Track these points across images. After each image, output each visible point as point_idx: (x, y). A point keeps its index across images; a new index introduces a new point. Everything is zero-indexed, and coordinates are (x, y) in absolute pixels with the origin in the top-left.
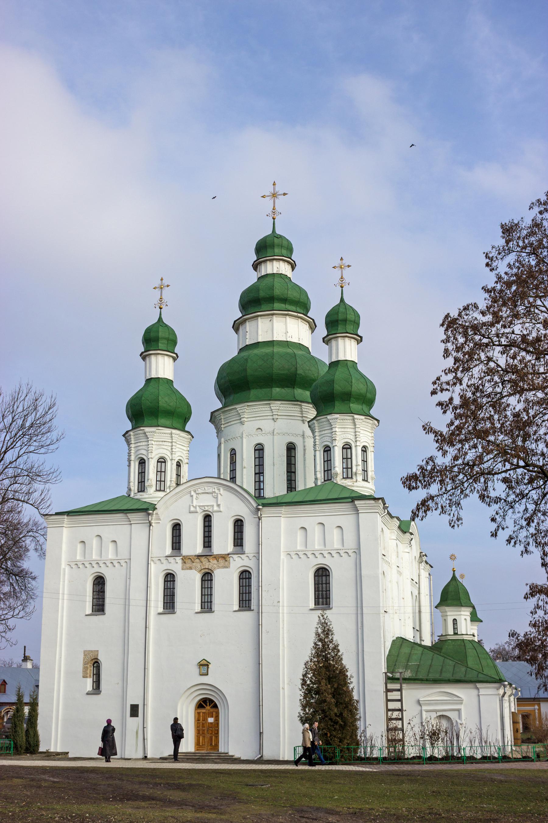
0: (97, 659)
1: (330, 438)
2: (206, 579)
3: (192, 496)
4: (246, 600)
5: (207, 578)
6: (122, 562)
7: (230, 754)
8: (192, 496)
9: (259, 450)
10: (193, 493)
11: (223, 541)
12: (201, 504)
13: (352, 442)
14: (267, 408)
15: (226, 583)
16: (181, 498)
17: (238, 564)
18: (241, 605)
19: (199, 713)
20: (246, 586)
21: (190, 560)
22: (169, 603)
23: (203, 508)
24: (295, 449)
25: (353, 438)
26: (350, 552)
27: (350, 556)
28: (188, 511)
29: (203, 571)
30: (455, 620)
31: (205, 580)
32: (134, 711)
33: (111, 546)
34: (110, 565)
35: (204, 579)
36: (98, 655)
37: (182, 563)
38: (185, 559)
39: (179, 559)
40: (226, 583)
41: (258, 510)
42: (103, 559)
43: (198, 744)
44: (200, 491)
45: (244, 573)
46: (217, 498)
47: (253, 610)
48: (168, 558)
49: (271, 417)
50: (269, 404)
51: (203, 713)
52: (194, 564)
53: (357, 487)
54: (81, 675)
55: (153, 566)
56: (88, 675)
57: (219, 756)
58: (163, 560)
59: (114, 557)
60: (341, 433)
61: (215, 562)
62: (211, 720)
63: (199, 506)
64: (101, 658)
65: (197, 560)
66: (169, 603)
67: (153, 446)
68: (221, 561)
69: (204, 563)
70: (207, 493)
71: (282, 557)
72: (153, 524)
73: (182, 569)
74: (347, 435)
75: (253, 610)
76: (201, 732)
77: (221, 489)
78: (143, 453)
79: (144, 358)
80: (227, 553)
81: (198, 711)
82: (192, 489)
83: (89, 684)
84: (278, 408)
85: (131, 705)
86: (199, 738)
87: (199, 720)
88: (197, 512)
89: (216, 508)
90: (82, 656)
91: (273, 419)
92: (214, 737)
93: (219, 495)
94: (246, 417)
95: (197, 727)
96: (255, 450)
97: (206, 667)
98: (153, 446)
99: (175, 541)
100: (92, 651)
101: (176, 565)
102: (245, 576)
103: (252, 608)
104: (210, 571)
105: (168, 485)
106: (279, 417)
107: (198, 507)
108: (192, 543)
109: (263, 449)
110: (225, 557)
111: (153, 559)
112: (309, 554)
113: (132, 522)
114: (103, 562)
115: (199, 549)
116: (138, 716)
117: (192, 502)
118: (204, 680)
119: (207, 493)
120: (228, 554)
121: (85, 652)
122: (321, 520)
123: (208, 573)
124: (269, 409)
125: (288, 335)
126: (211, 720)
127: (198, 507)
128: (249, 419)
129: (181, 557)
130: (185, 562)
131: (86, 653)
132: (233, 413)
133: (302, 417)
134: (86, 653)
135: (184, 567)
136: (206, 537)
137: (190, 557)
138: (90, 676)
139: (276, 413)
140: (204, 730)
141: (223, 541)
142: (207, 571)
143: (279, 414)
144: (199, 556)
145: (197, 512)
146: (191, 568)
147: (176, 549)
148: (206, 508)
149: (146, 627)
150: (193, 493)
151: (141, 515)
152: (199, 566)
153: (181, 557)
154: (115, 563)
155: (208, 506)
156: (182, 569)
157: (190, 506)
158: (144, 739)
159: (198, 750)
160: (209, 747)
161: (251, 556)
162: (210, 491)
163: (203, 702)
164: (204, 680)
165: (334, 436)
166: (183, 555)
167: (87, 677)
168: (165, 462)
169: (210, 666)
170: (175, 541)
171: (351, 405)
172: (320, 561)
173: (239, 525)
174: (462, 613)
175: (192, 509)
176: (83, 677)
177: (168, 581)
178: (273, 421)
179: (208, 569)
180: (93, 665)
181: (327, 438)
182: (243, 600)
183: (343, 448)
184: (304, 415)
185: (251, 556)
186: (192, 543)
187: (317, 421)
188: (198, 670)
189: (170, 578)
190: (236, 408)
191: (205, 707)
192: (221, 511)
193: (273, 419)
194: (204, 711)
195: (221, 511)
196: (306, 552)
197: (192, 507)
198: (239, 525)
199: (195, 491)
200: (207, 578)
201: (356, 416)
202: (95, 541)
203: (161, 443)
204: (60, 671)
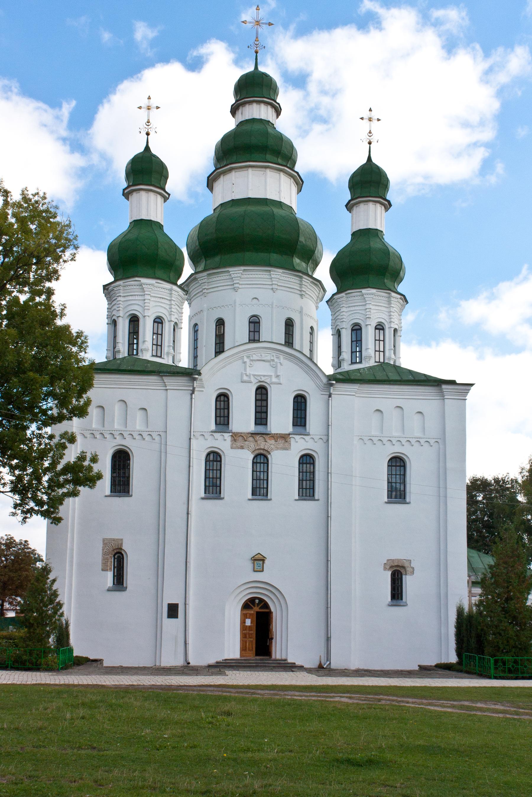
0: (121, 549)
1: (362, 316)
2: (259, 461)
3: (245, 363)
4: (306, 489)
5: (261, 460)
6: (154, 435)
7: (290, 660)
8: (245, 363)
9: (255, 323)
10: (246, 359)
11: (280, 418)
12: (256, 374)
13: (386, 323)
14: (265, 275)
15: (284, 468)
16: (231, 363)
17: (300, 445)
18: (301, 494)
20: (306, 472)
21: (241, 438)
22: (213, 487)
23: (259, 378)
24: (293, 326)
25: (386, 317)
26: (432, 441)
27: (431, 446)
28: (240, 381)
29: (257, 452)
31: (257, 463)
32: (173, 611)
33: (140, 415)
34: (138, 437)
35: (255, 461)
36: (122, 544)
37: (231, 441)
38: (235, 436)
39: (227, 436)
40: (284, 468)
41: (332, 385)
42: (129, 428)
43: (243, 649)
44: (255, 357)
45: (305, 457)
46: (275, 367)
47: (318, 500)
48: (213, 434)
49: (271, 287)
50: (270, 271)
52: (247, 443)
54: (100, 567)
56: (109, 568)
57: (279, 663)
58: (207, 435)
59: (143, 428)
60: (375, 311)
61: (273, 442)
63: (254, 375)
64: (125, 547)
65: (251, 439)
66: (213, 487)
67: (151, 302)
68: (281, 442)
69: (259, 442)
70: (264, 361)
71: (355, 442)
72: (196, 393)
73: (232, 448)
74: (381, 314)
75: (318, 500)
76: (248, 636)
77: (282, 357)
78: (136, 310)
80: (287, 433)
81: (244, 612)
82: (245, 354)
83: (109, 577)
84: (278, 277)
85: (169, 604)
86: (246, 642)
88: (251, 382)
89: (274, 380)
90: (100, 545)
91: (272, 289)
93: (279, 364)
94: (241, 283)
96: (250, 322)
97: (261, 562)
98: (151, 302)
99: (218, 415)
100: (114, 540)
101: (223, 443)
102: (307, 460)
103: (316, 497)
104: (265, 453)
105: (166, 351)
106: (279, 288)
107: (252, 376)
108: (243, 417)
109: (259, 323)
110: (285, 437)
111: (195, 434)
112: (385, 440)
113: (168, 388)
114: (129, 433)
115: (251, 427)
116: (177, 617)
117: (245, 369)
118: (259, 576)
119: (264, 361)
120: (289, 434)
121: (104, 540)
122: (399, 403)
123: (261, 454)
124: (268, 277)
125: (282, 195)
127: (252, 376)
128: (244, 286)
129: (231, 434)
130: (235, 440)
131: (106, 542)
132: (224, 276)
133: (301, 291)
134: (106, 542)
135: (234, 446)
136: (259, 412)
137: (242, 435)
138: (110, 569)
139: (276, 283)
140: (251, 634)
141: (280, 418)
142: (262, 452)
143: (279, 284)
144: (253, 434)
145: (251, 382)
146: (242, 448)
147: (220, 424)
148: (263, 379)
149: (188, 514)
150: (246, 359)
151: (182, 381)
152: (252, 445)
153: (231, 434)
154: (145, 435)
155: (264, 376)
156: (232, 448)
157: (242, 375)
158: (186, 643)
161: (316, 438)
162: (268, 358)
163: (250, 601)
164: (259, 576)
165: (367, 313)
166: (234, 431)
167: (107, 570)
168: (162, 323)
169: (266, 561)
170: (218, 415)
171: (386, 281)
172: (396, 449)
173: (300, 403)
175: (245, 378)
176: (103, 570)
177: (210, 461)
178: (271, 291)
179: (264, 449)
180: (114, 556)
181: (360, 315)
182: (303, 488)
183: (352, 330)
184: (303, 289)
185: (316, 438)
186: (243, 417)
187: (346, 294)
189: (214, 459)
190: (229, 272)
191: (252, 608)
192: (280, 384)
193: (272, 289)
195: (280, 384)
196: (381, 438)
197: (244, 375)
198: (300, 403)
199: (248, 357)
200: (261, 460)
201: (393, 294)
202: (118, 408)
203: (159, 300)
204: (71, 562)
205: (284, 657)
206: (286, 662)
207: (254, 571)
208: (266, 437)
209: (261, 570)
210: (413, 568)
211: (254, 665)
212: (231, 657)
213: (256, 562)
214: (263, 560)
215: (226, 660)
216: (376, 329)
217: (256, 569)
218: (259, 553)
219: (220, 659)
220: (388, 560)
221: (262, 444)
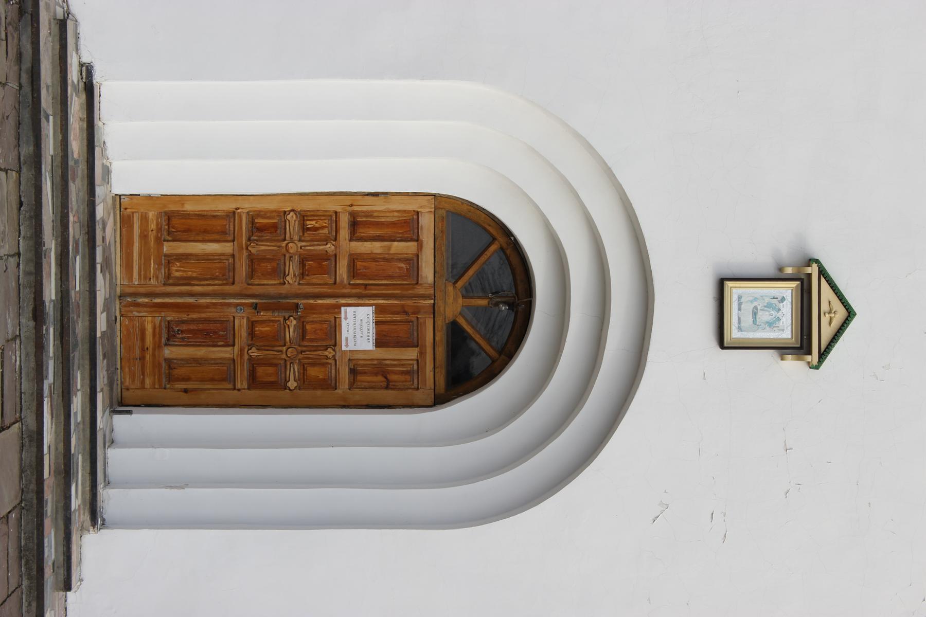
19: (407, 227)
43: (179, 219)
51: (414, 262)
57: (66, 473)
62: (358, 328)
76: (265, 247)
81: (427, 222)
86: (221, 235)
87: (354, 225)
92: (223, 353)
95: (303, 217)
97: (786, 331)
118: (682, 315)
126: (358, 328)
140: (279, 273)
159: (126, 221)
160: (150, 322)
169: (793, 366)
188: (763, 262)
194: (427, 272)
205: (112, 500)
206: (80, 516)
207: (721, 284)
209: (733, 333)
211: (50, 292)
212: (113, 129)
213: (787, 291)
214: (805, 344)
215: (89, 89)
217: (734, 290)
218: (850, 314)
219: (92, 46)
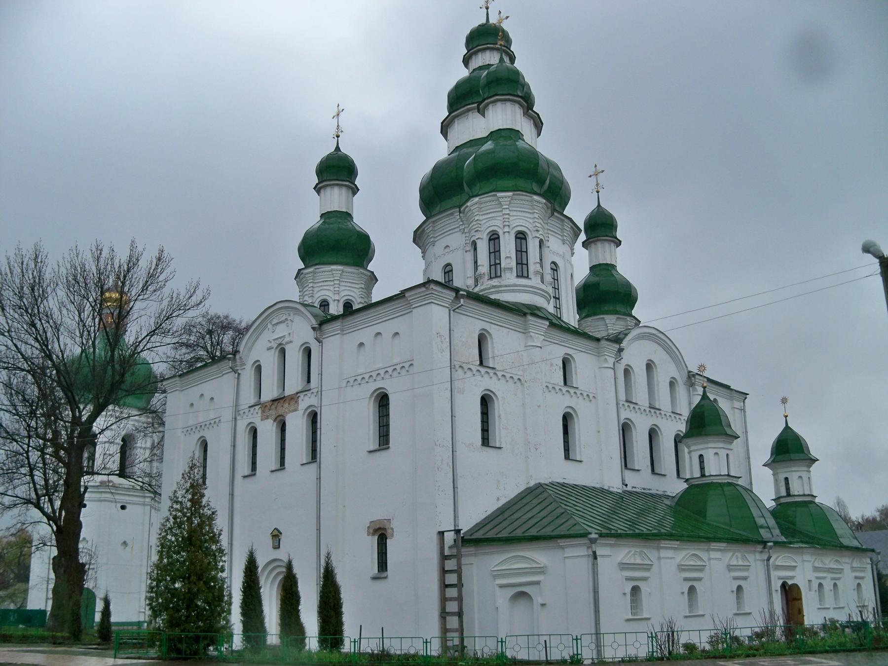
16: (260, 334)
30: (701, 456)
44: (275, 321)
53: (506, 286)
55: (239, 423)
58: (247, 411)
61: (286, 405)
79: (318, 192)
89: (287, 339)
102: (314, 418)
146: (267, 418)
155: (280, 338)
162: (283, 319)
169: (283, 538)
174: (710, 445)
192: (291, 342)
201: (499, 194)
208: (281, 401)
210: (392, 529)
216: (516, 238)
220: (371, 522)
221: (281, 411)
